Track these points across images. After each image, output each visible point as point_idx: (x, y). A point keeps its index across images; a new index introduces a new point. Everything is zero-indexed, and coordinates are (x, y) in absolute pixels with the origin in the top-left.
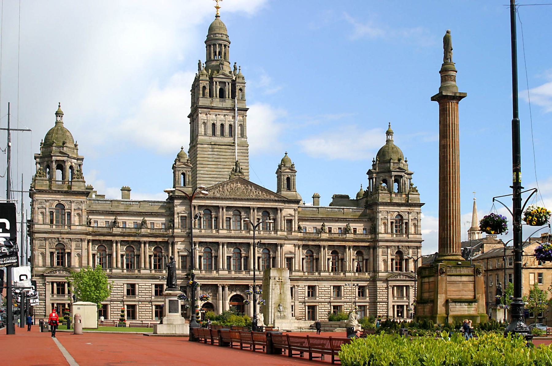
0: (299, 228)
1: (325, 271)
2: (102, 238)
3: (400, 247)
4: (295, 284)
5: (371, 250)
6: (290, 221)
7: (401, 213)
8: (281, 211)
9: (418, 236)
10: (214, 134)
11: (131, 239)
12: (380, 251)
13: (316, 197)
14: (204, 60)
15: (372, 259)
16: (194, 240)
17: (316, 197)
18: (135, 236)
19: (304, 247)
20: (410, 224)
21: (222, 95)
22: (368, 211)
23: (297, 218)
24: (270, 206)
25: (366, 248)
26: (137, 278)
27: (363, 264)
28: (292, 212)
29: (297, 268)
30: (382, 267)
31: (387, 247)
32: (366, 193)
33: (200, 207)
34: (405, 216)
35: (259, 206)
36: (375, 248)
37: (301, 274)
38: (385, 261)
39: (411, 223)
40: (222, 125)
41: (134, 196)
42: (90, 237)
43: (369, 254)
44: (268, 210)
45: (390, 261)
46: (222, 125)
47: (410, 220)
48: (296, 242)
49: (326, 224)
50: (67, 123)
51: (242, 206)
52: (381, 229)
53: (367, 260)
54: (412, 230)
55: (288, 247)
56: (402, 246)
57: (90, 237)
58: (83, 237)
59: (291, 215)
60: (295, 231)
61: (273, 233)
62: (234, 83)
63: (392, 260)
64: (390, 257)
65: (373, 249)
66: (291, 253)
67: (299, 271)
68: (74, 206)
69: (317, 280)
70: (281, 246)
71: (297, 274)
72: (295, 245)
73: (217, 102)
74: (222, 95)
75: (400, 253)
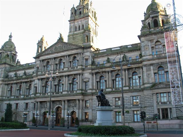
3: (160, 63)
4: (90, 98)
5: (141, 69)
6: (87, 60)
16: (39, 77)
18: (20, 80)
23: (90, 57)
26: (18, 100)
29: (90, 88)
31: (152, 65)
33: (43, 60)
35: (69, 54)
37: (94, 91)
45: (153, 74)
48: (90, 71)
49: (110, 57)
50: (13, 40)
51: (61, 56)
56: (161, 62)
57: (6, 83)
60: (89, 65)
64: (152, 72)
66: (86, 78)
67: (93, 89)
71: (90, 91)
72: (90, 73)
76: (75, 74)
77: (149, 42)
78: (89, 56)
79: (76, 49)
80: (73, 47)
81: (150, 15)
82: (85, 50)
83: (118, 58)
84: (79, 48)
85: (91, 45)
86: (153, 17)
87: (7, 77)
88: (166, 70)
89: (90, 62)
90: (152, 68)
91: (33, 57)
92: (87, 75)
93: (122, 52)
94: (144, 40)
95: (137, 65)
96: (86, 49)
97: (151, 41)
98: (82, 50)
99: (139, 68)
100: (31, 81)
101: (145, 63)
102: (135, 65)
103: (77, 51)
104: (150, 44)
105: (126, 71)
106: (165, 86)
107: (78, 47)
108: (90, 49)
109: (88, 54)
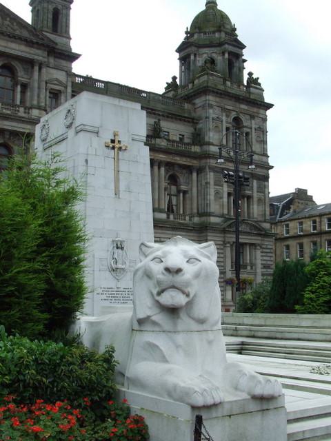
5: (195, 175)
7: (242, 117)
8: (40, 69)
9: (264, 159)
12: (211, 177)
15: (195, 190)
20: (254, 134)
22: (186, 106)
24: (19, 54)
25: (184, 171)
27: (178, 200)
28: (61, 76)
30: (214, 208)
34: (246, 121)
36: (200, 171)
39: (254, 135)
43: (189, 182)
44: (15, 63)
45: (225, 195)
47: (253, 130)
52: (212, 136)
53: (185, 193)
54: (256, 147)
59: (60, 83)
61: (22, 109)
63: (229, 194)
65: (198, 174)
77: (224, 114)
78: (66, 87)
79: (29, 43)
80: (16, 27)
81: (228, 44)
82: (52, 60)
84: (43, 45)
85: (74, 51)
86: (230, 53)
88: (248, 192)
91: (273, 105)
94: (214, 103)
95: (188, 160)
96: (55, 57)
98: (45, 54)
99: (189, 169)
101: (212, 162)
102: (184, 159)
103: (27, 49)
104: (224, 118)
105: (163, 169)
106: (248, 230)
107: (40, 42)
108: (69, 63)
109: (61, 76)
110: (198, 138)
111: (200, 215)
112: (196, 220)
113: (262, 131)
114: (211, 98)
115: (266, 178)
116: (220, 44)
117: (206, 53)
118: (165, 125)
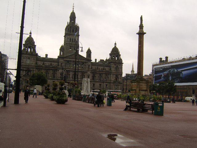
0: (92, 67)
1: (97, 80)
2: (40, 68)
6: (89, 66)
10: (70, 41)
11: (47, 68)
12: (112, 75)
13: (96, 60)
14: (69, 22)
17: (96, 60)
19: (93, 73)
21: (73, 31)
31: (114, 74)
32: (109, 59)
36: (110, 74)
38: (113, 78)
40: (73, 39)
41: (49, 57)
42: (37, 67)
46: (73, 39)
52: (112, 69)
54: (120, 70)
55: (89, 73)
57: (37, 67)
58: (35, 67)
62: (76, 29)
64: (114, 77)
68: (32, 58)
69: (95, 82)
70: (87, 72)
73: (72, 33)
74: (73, 31)
75: (117, 76)
76: (83, 72)
79: (85, 60)
83: (101, 68)
87: (36, 63)
89: (90, 67)
90: (114, 75)
92: (89, 73)
93: (103, 66)
97: (115, 65)
99: (109, 74)
100: (57, 70)
109: (90, 63)
110: (110, 69)
111: (110, 80)
112: (109, 81)
113: (122, 67)
114: (112, 64)
115: (122, 75)
116: (115, 54)
117: (113, 55)
118: (105, 68)
